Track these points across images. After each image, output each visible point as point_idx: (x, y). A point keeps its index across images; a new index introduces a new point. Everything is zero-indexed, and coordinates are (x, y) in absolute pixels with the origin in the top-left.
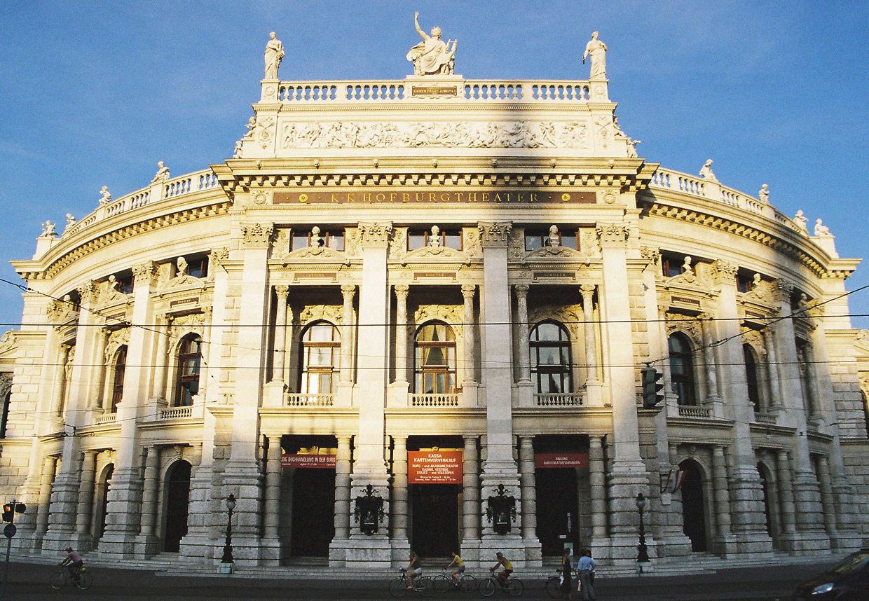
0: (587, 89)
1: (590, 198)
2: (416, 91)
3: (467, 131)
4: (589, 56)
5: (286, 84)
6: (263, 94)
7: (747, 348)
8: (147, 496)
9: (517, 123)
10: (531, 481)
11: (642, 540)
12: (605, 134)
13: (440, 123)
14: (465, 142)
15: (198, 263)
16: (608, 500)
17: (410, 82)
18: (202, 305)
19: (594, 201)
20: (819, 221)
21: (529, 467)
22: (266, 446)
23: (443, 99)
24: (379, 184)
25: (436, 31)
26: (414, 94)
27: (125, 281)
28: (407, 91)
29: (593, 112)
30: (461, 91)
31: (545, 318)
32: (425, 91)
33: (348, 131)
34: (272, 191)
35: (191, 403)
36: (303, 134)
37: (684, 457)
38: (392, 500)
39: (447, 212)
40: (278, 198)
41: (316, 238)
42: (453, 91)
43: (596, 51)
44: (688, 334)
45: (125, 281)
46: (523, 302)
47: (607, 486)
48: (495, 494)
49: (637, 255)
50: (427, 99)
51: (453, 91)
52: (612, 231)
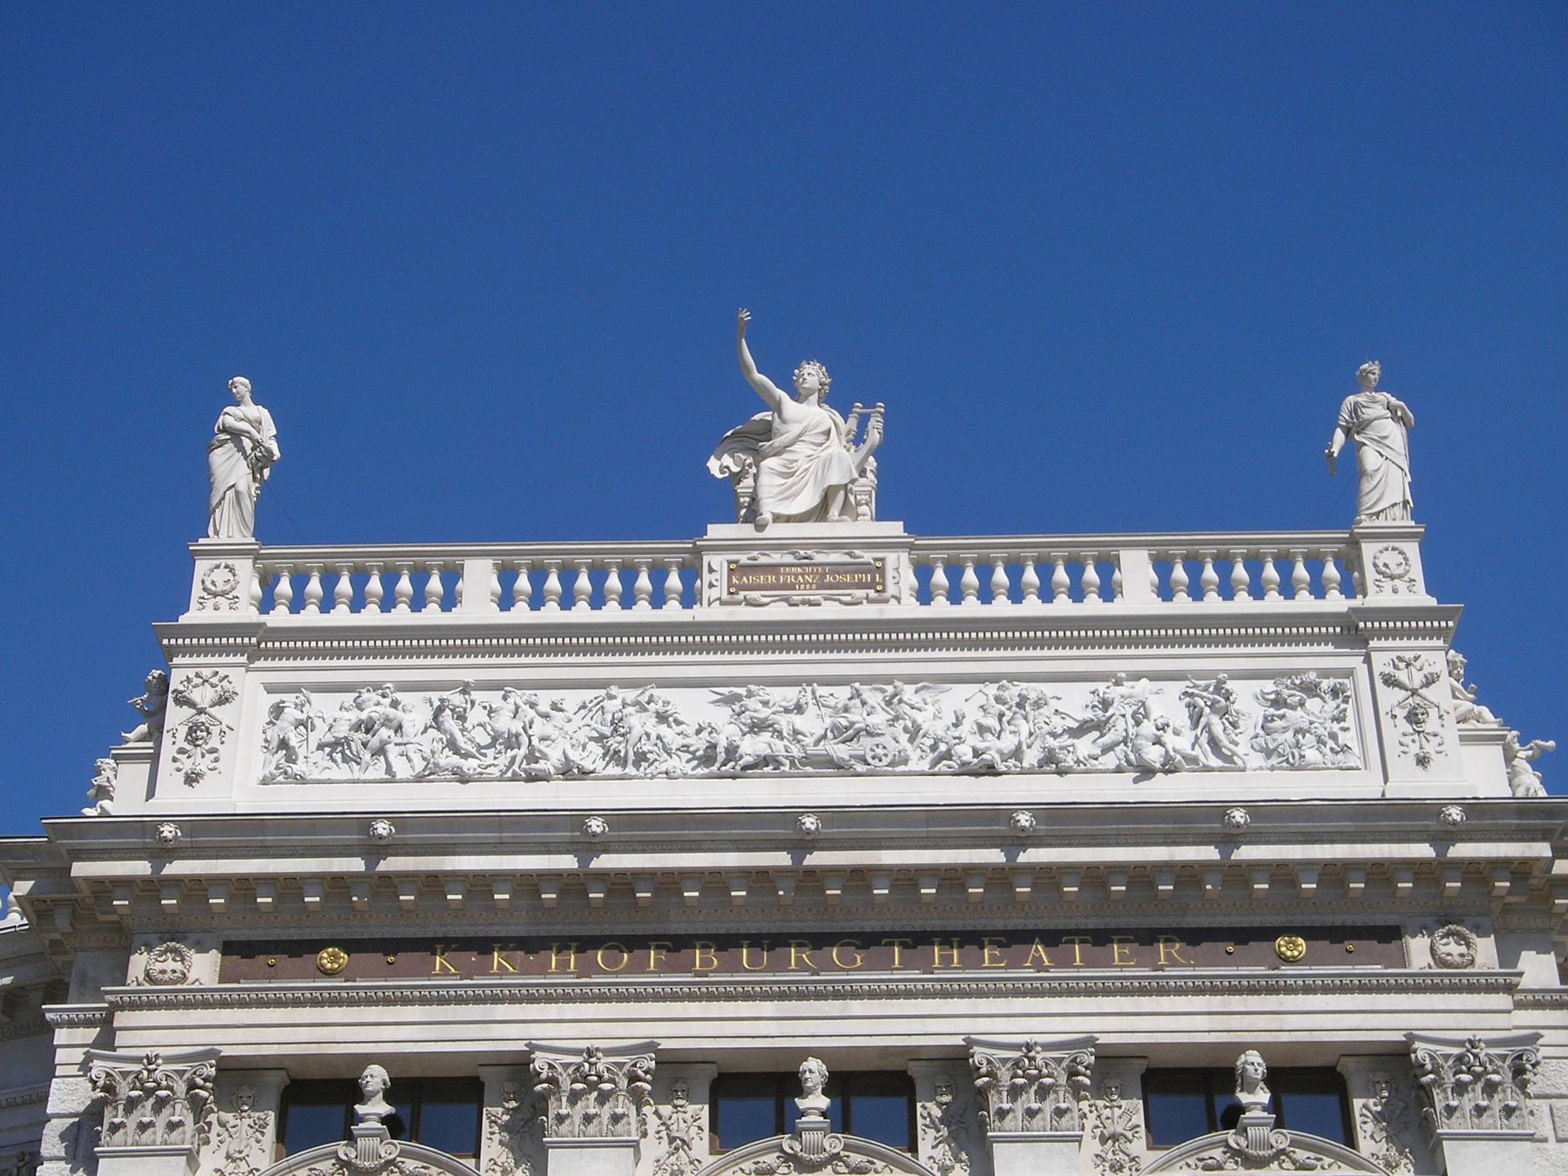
3: (919, 717)
4: (1352, 450)
6: (197, 591)
9: (1101, 687)
13: (822, 691)
14: (914, 754)
25: (812, 374)
26: (733, 589)
29: (1373, 643)
32: (771, 579)
33: (505, 723)
36: (342, 731)
39: (856, 1007)
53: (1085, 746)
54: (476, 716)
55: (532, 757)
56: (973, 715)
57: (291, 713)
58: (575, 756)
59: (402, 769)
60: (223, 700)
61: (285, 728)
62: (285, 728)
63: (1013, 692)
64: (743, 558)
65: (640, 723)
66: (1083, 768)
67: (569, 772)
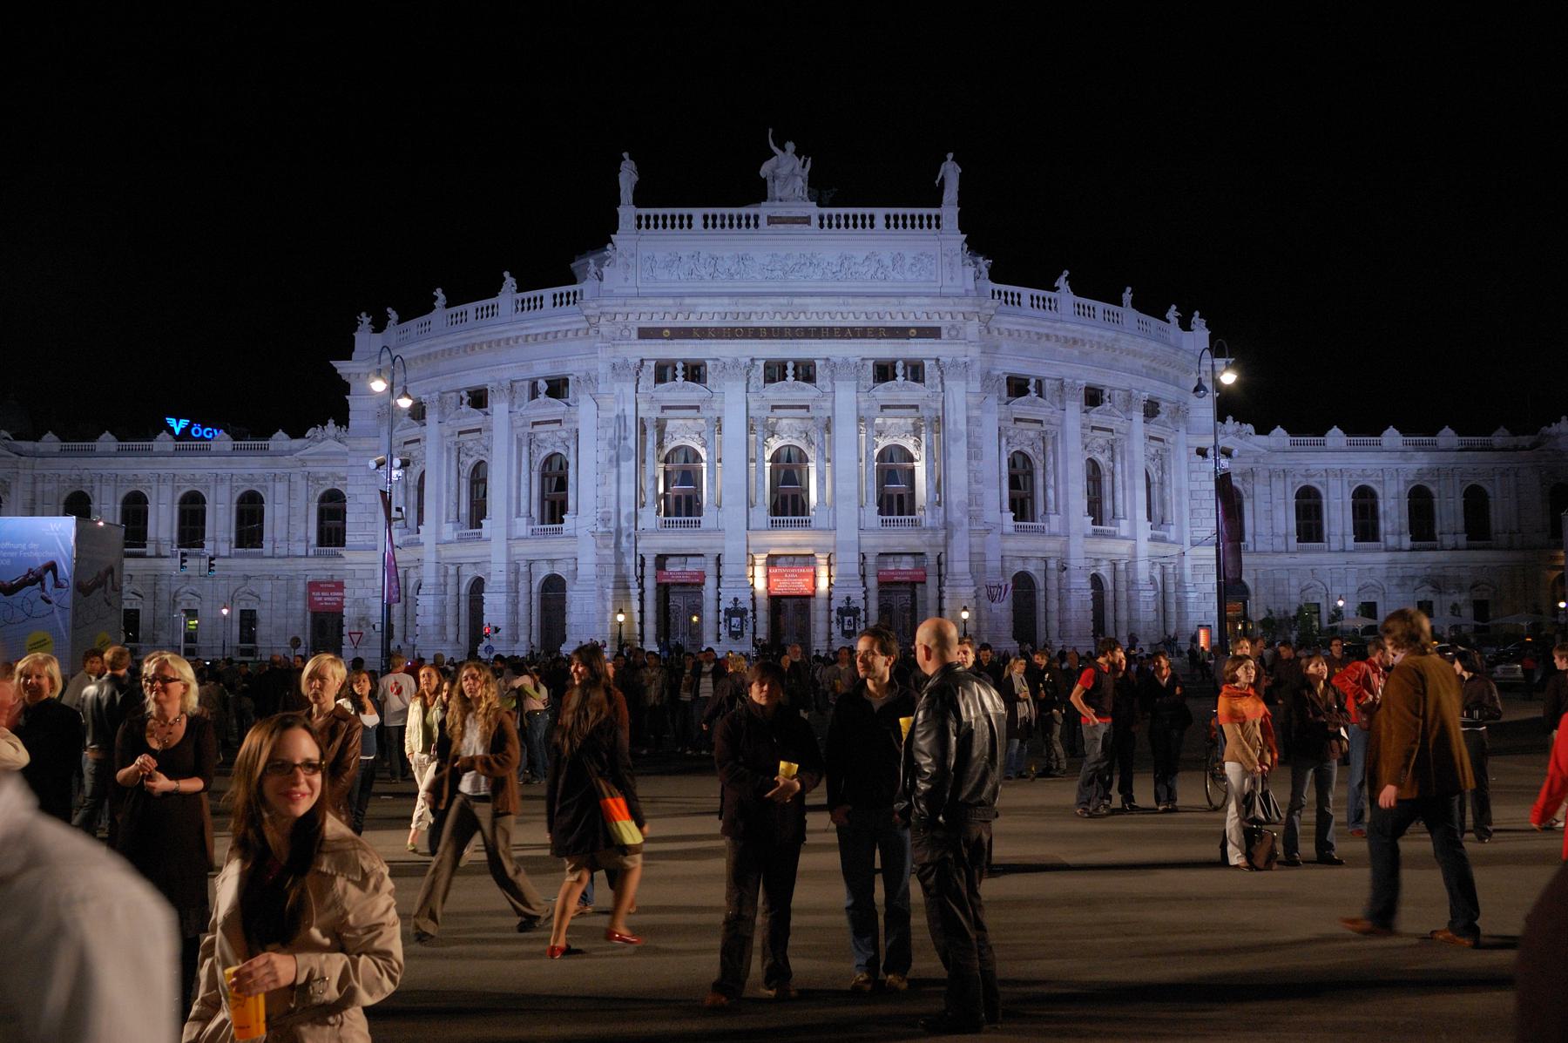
0: (938, 218)
2: (772, 220)
5: (644, 212)
8: (522, 607)
10: (873, 595)
15: (557, 388)
17: (764, 210)
20: (1197, 313)
21: (872, 582)
22: (643, 565)
27: (478, 399)
28: (763, 221)
30: (815, 221)
38: (754, 610)
43: (951, 172)
47: (941, 598)
48: (843, 605)
52: (955, 364)
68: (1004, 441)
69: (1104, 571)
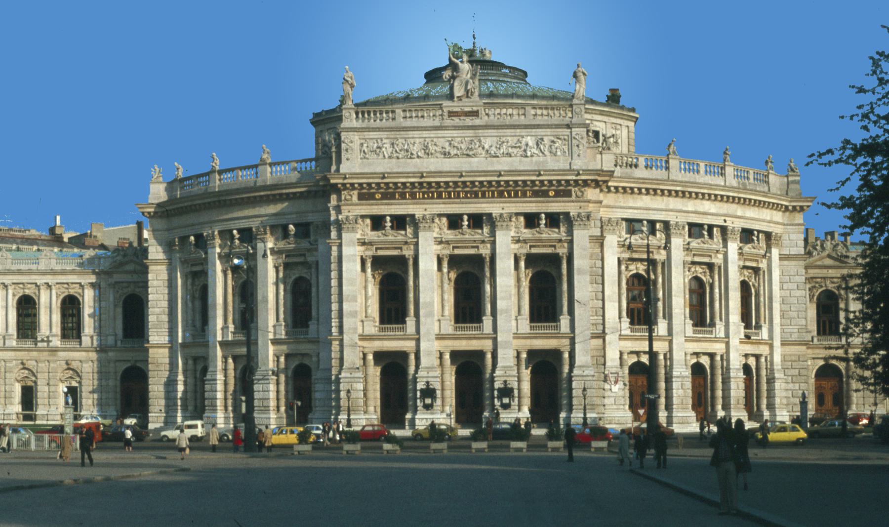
1: (568, 194)
2: (452, 114)
7: (697, 279)
11: (585, 414)
12: (578, 146)
16: (570, 389)
18: (310, 259)
19: (570, 196)
23: (469, 121)
24: (429, 189)
26: (449, 116)
27: (248, 235)
31: (539, 269)
33: (406, 147)
34: (356, 192)
35: (307, 326)
37: (634, 359)
40: (361, 197)
41: (389, 224)
42: (475, 114)
44: (644, 273)
45: (248, 235)
46: (522, 264)
48: (502, 386)
49: (597, 232)
50: (456, 121)
51: (475, 114)
53: (515, 151)
54: (400, 145)
55: (412, 154)
56: (494, 145)
57: (365, 145)
58: (419, 154)
59: (387, 156)
60: (351, 142)
61: (365, 148)
62: (365, 148)
63: (504, 139)
64: (450, 109)
65: (432, 148)
66: (516, 156)
67: (418, 157)
68: (623, 267)
69: (705, 361)
